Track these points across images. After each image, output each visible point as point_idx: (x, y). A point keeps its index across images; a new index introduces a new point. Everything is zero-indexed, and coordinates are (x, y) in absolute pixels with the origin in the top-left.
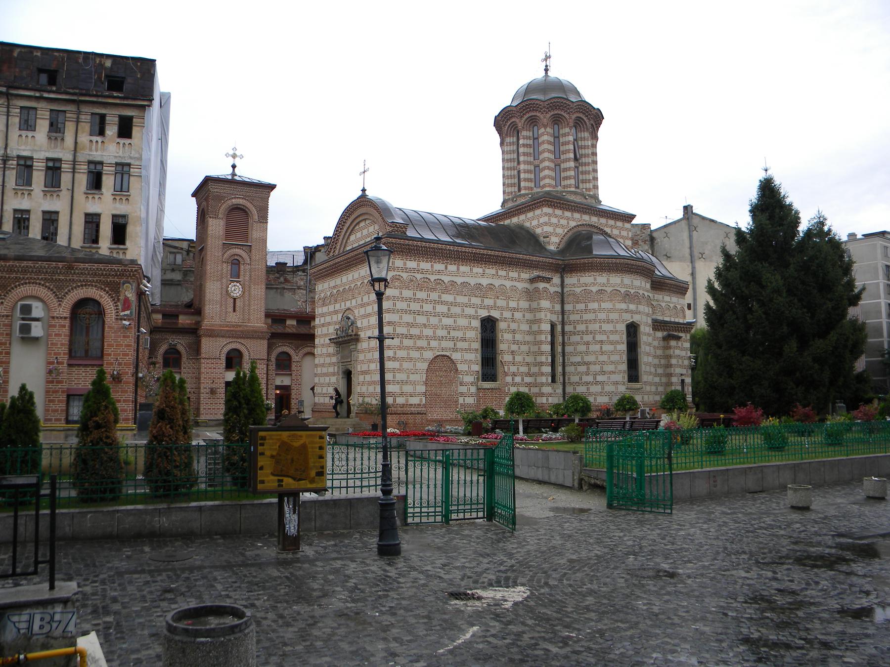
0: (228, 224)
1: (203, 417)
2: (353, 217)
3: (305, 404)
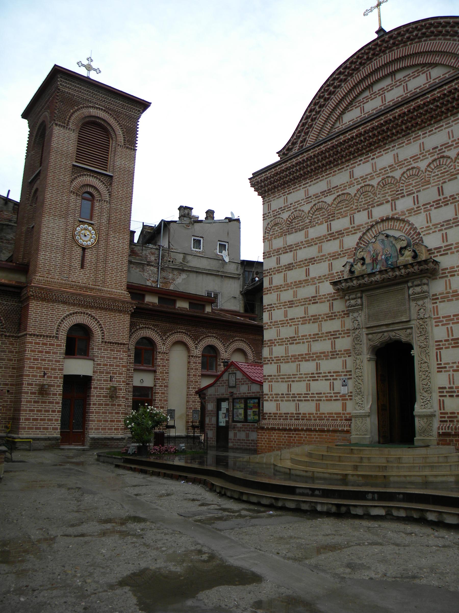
0: (80, 141)
1: (24, 434)
2: (357, 77)
3: (177, 414)
